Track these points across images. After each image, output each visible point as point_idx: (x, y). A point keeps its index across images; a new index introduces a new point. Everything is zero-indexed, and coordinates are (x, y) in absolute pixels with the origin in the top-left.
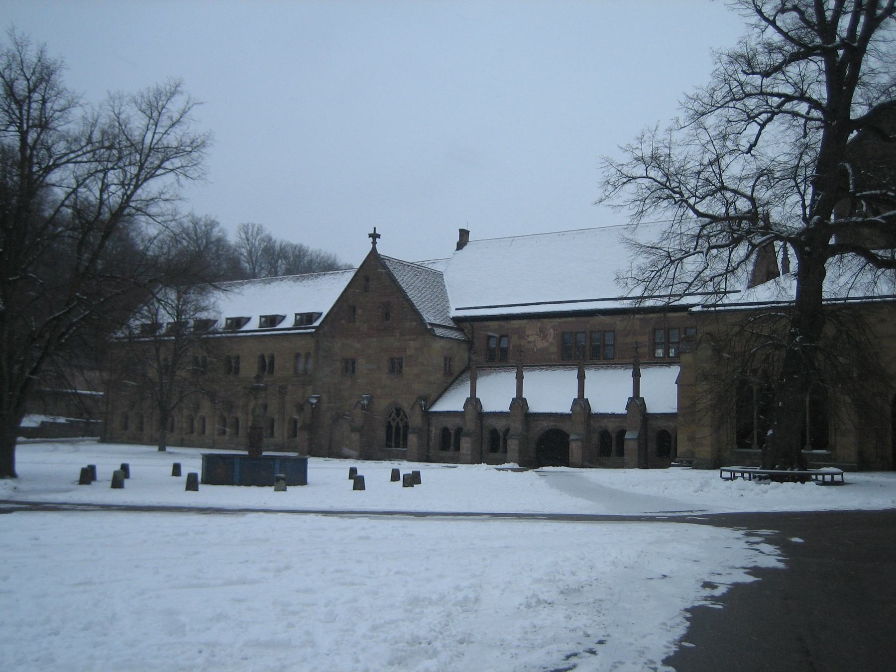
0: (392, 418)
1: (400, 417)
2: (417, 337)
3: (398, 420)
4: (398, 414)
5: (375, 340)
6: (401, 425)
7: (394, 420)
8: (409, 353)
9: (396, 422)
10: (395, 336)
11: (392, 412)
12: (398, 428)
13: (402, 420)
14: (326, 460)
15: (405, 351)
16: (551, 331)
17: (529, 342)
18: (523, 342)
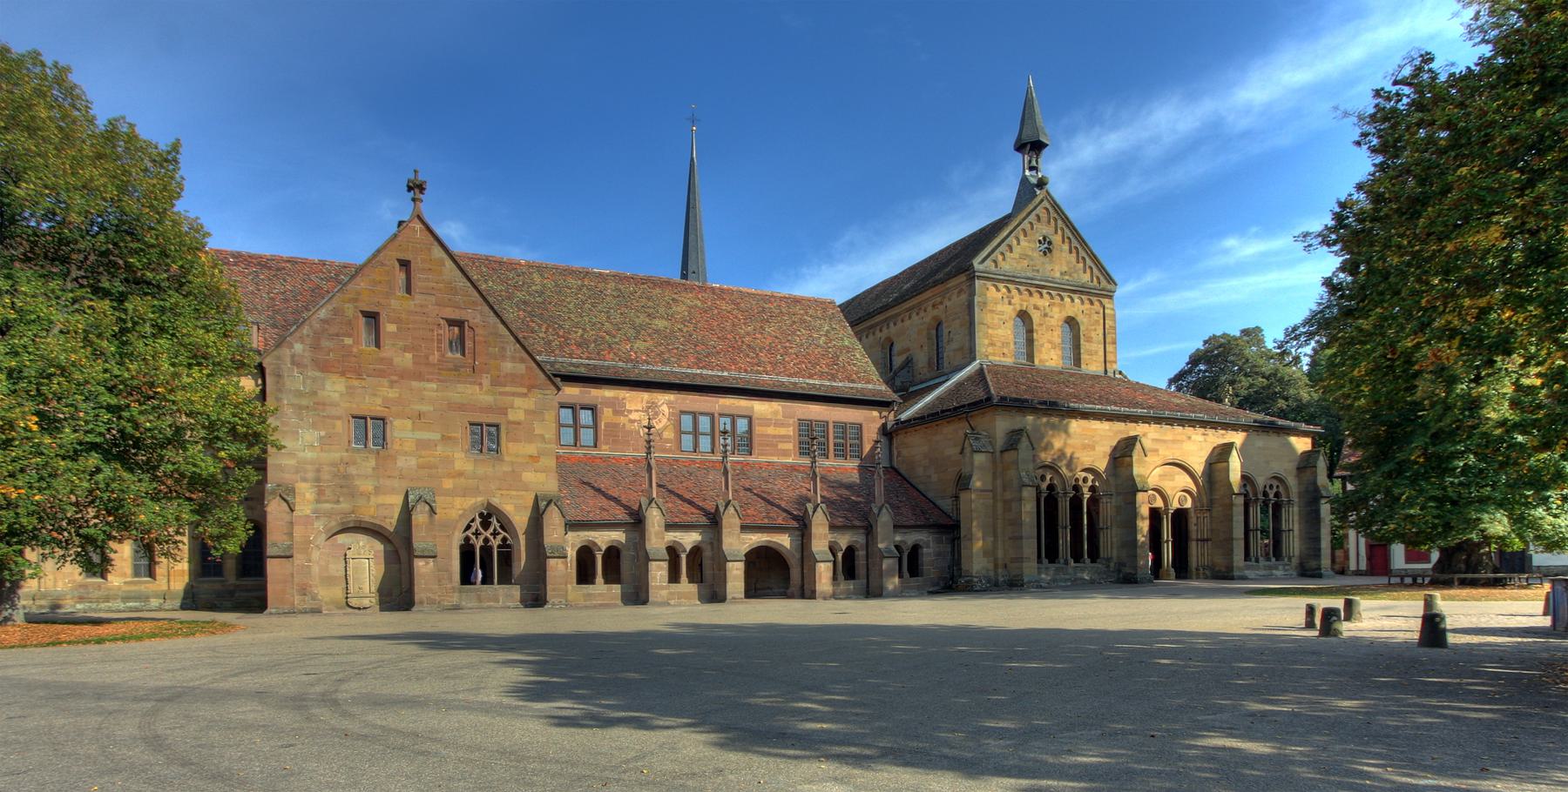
0: (473, 530)
1: (491, 530)
2: (529, 390)
3: (488, 534)
4: (486, 524)
5: (434, 386)
6: (495, 543)
7: (477, 534)
8: (512, 416)
9: (481, 538)
10: (481, 384)
11: (473, 521)
12: (486, 549)
13: (495, 534)
14: (344, 614)
15: (506, 414)
16: (665, 408)
17: (633, 421)
18: (622, 420)
